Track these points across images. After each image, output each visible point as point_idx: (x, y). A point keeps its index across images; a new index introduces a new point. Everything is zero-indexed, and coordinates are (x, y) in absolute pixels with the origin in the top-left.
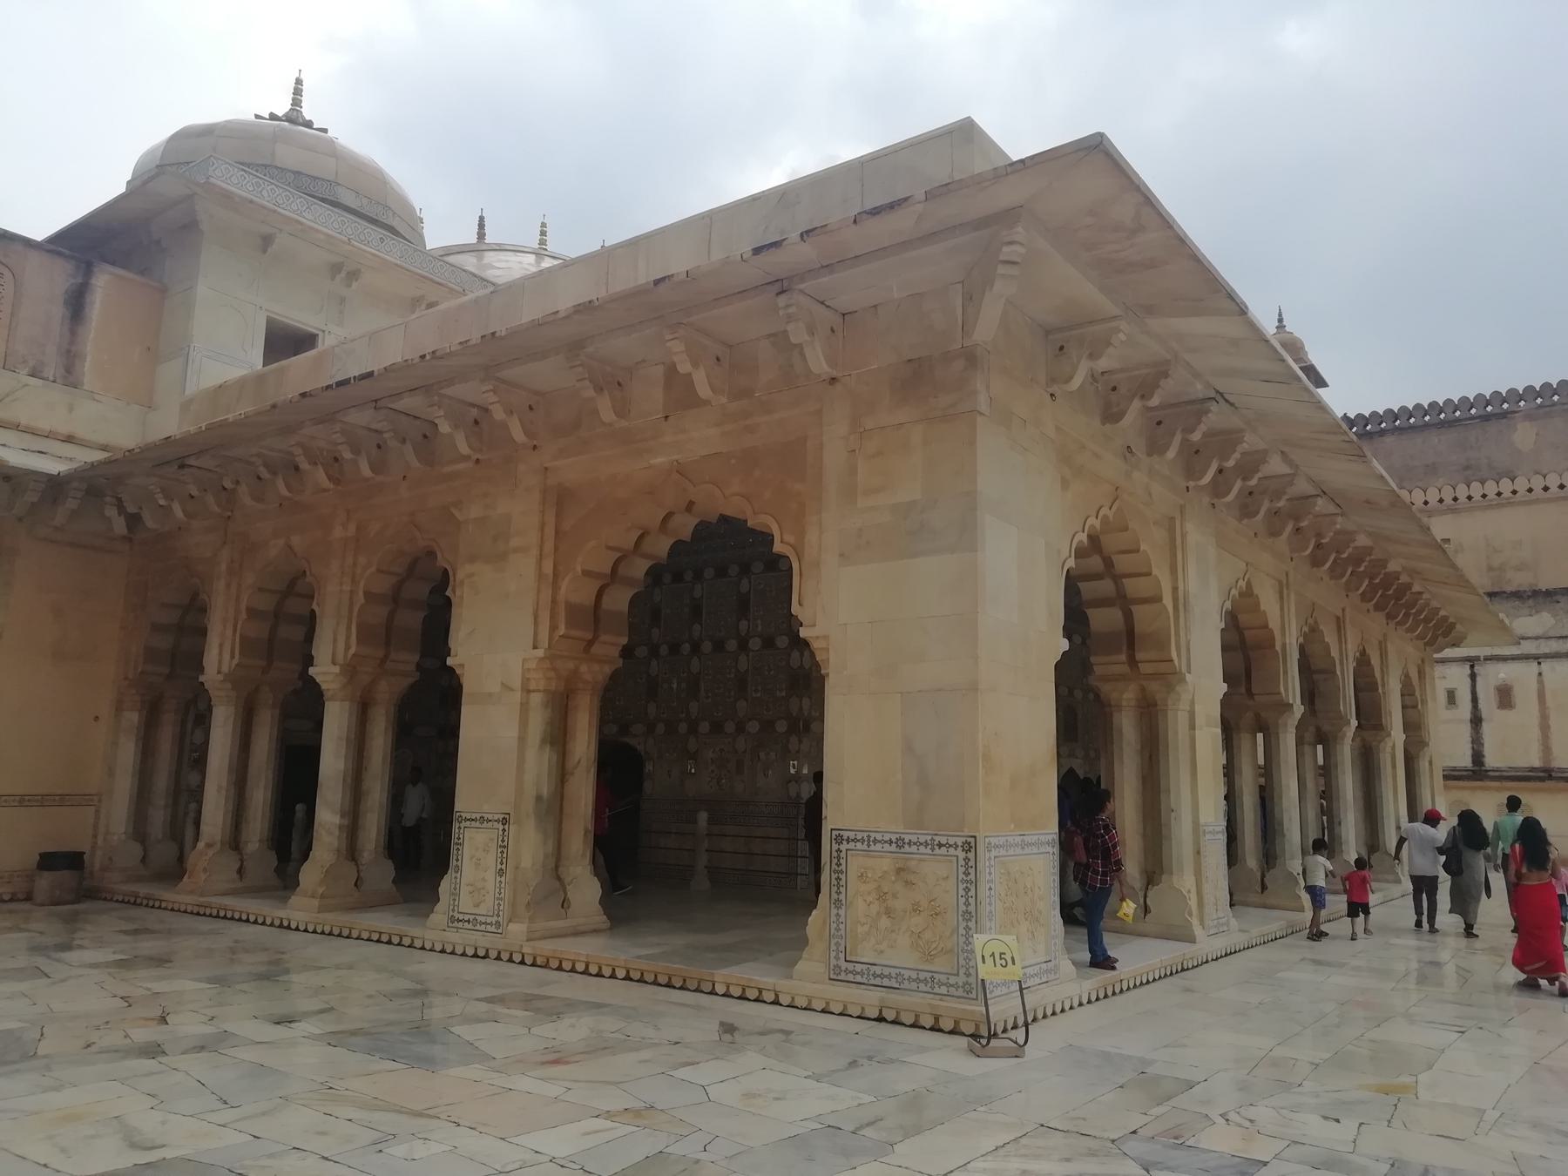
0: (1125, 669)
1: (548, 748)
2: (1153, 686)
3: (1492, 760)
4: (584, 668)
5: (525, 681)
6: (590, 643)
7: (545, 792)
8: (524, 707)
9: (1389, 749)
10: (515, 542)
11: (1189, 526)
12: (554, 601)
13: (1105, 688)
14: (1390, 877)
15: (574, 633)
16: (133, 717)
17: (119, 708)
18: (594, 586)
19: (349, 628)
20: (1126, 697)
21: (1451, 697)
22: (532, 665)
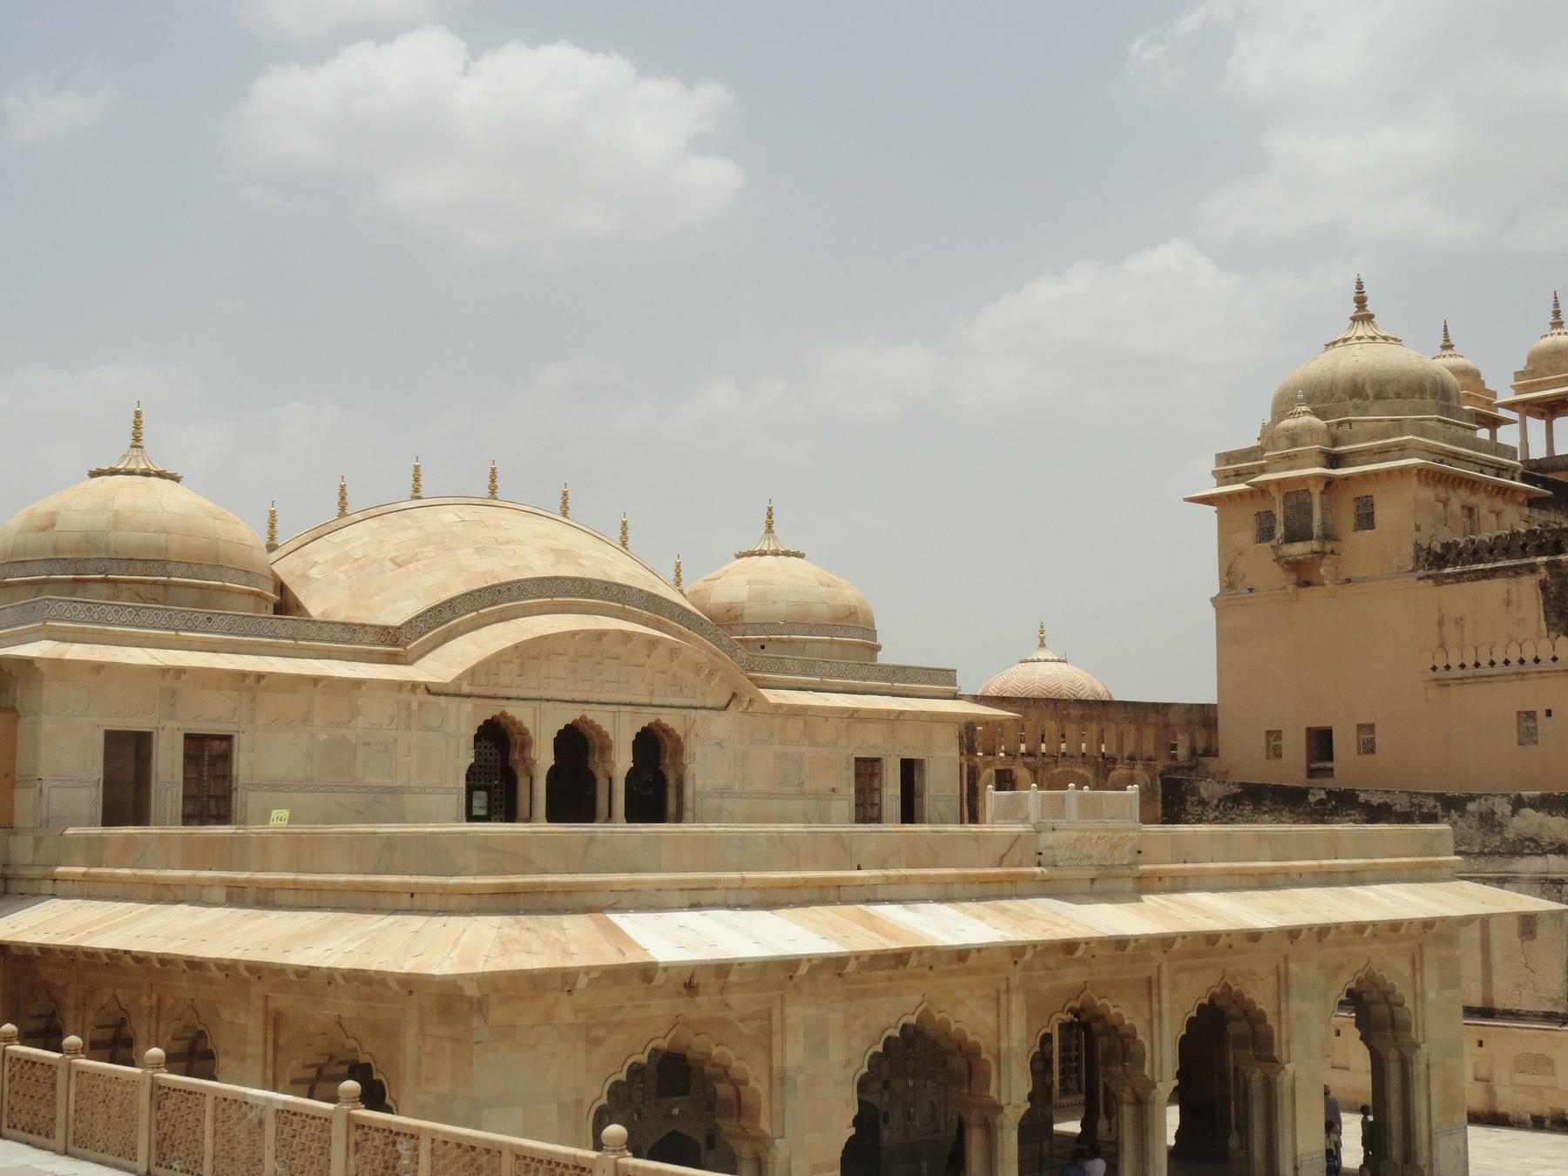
11: (789, 1011)
13: (731, 1142)
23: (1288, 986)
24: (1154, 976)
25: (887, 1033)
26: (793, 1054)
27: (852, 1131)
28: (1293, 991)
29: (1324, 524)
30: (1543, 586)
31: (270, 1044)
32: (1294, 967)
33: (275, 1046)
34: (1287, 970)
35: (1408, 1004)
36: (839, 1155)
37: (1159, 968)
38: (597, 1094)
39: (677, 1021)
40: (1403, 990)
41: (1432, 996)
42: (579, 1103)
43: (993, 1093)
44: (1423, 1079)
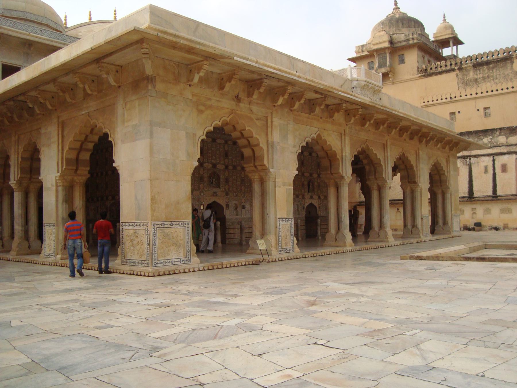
0: (254, 168)
1: (64, 203)
2: (262, 174)
3: (499, 192)
4: (75, 178)
5: (57, 183)
6: (77, 170)
8: (57, 191)
9: (419, 190)
10: (52, 140)
11: (274, 119)
12: (62, 158)
13: (250, 175)
14: (417, 236)
15: (70, 167)
19: (18, 169)
20: (255, 177)
21: (486, 168)
22: (57, 178)
23: (419, 158)
24: (385, 143)
25: (307, 139)
26: (276, 137)
27: (297, 173)
29: (390, 62)
30: (457, 75)
31: (60, 136)
32: (421, 152)
33: (63, 136)
35: (446, 174)
36: (293, 179)
37: (387, 141)
39: (232, 112)
40: (445, 169)
41: (452, 173)
42: (194, 135)
43: (340, 171)
44: (450, 198)
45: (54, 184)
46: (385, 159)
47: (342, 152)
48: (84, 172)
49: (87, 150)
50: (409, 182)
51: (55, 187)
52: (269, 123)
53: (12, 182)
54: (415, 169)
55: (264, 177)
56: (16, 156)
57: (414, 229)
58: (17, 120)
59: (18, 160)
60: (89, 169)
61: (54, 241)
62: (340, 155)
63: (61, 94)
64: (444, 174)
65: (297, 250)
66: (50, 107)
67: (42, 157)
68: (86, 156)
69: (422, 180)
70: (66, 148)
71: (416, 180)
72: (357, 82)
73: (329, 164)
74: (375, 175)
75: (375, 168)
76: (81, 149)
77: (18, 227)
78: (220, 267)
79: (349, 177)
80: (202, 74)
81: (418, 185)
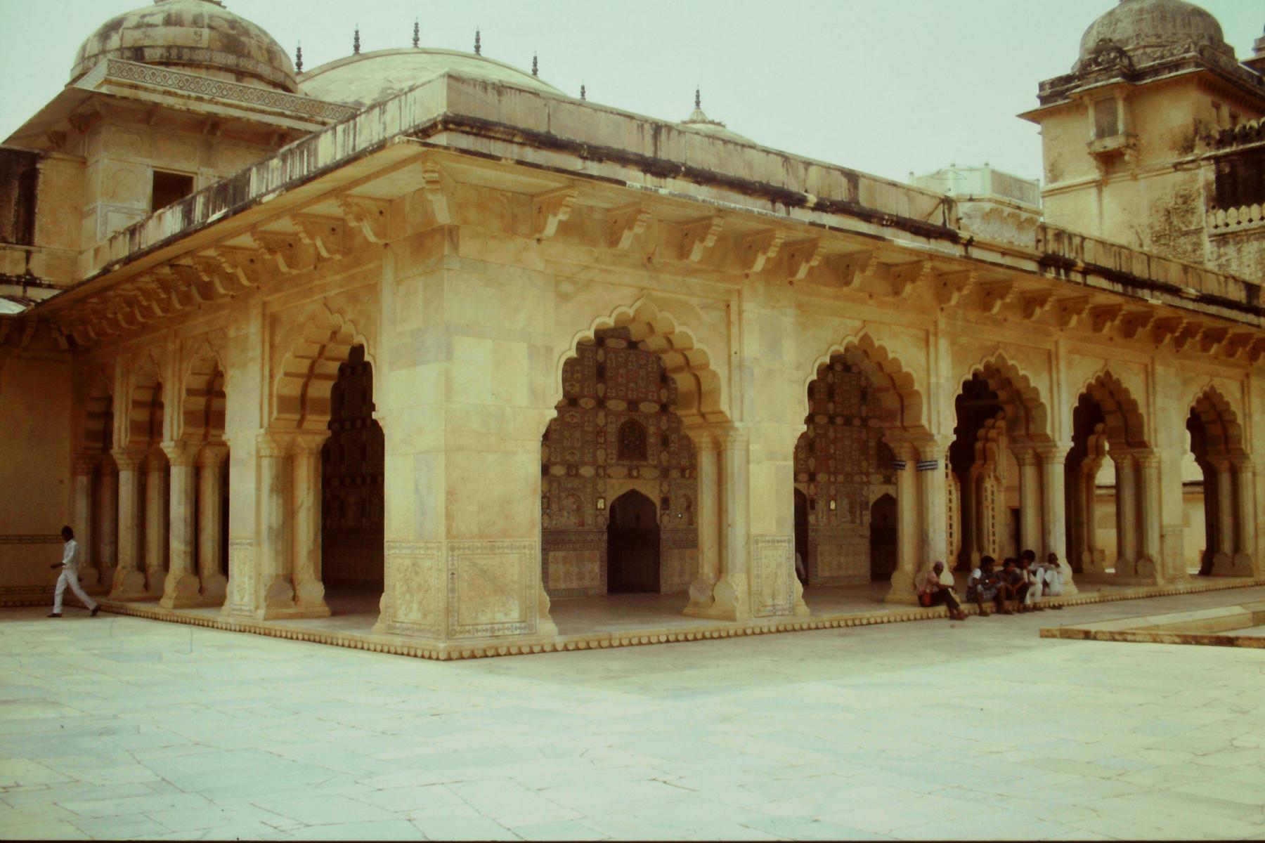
0: (699, 420)
1: (275, 495)
2: (718, 432)
4: (300, 439)
5: (258, 451)
7: (275, 526)
8: (259, 467)
9: (1154, 465)
10: (251, 354)
11: (747, 306)
12: (271, 395)
13: (691, 434)
14: (1149, 581)
15: (288, 416)
16: (83, 480)
17: (74, 474)
18: (300, 381)
20: (702, 440)
22: (260, 439)
23: (1154, 383)
24: (1053, 350)
25: (834, 348)
26: (751, 346)
28: (1159, 388)
32: (1159, 369)
33: (272, 346)
34: (1153, 370)
35: (1240, 421)
37: (1056, 343)
38: (566, 346)
41: (1256, 417)
42: (549, 349)
45: (254, 453)
46: (1051, 390)
47: (929, 376)
48: (319, 426)
49: (327, 377)
50: (1129, 444)
51: (253, 462)
52: (734, 317)
53: (168, 446)
54: (1142, 410)
55: (721, 439)
56: (177, 386)
57: (1141, 562)
58: (178, 306)
59: (179, 395)
60: (328, 418)
61: (250, 578)
62: (925, 384)
63: (268, 257)
64: (1233, 422)
65: (803, 609)
66: (245, 282)
67: (228, 390)
68: (322, 390)
69: (1162, 438)
70: (279, 376)
71: (1146, 438)
72: (970, 204)
73: (897, 405)
74: (1027, 428)
75: (1028, 411)
76: (311, 375)
77: (178, 546)
78: (605, 643)
79: (946, 437)
80: (562, 217)
81: (1152, 452)
